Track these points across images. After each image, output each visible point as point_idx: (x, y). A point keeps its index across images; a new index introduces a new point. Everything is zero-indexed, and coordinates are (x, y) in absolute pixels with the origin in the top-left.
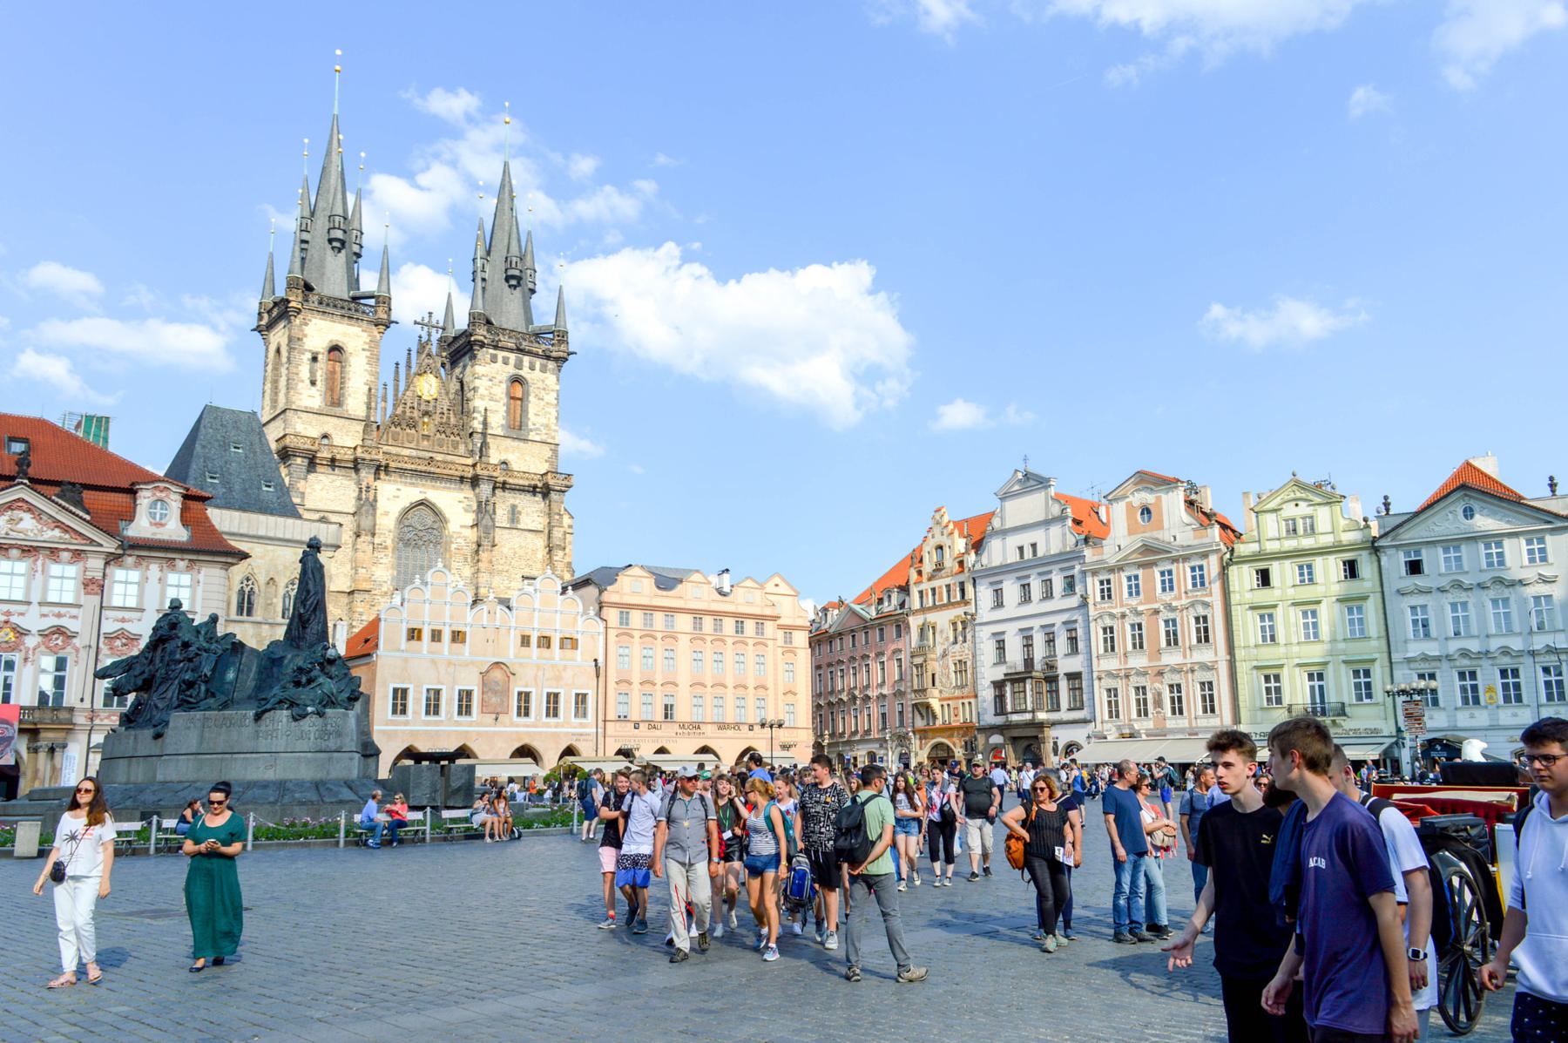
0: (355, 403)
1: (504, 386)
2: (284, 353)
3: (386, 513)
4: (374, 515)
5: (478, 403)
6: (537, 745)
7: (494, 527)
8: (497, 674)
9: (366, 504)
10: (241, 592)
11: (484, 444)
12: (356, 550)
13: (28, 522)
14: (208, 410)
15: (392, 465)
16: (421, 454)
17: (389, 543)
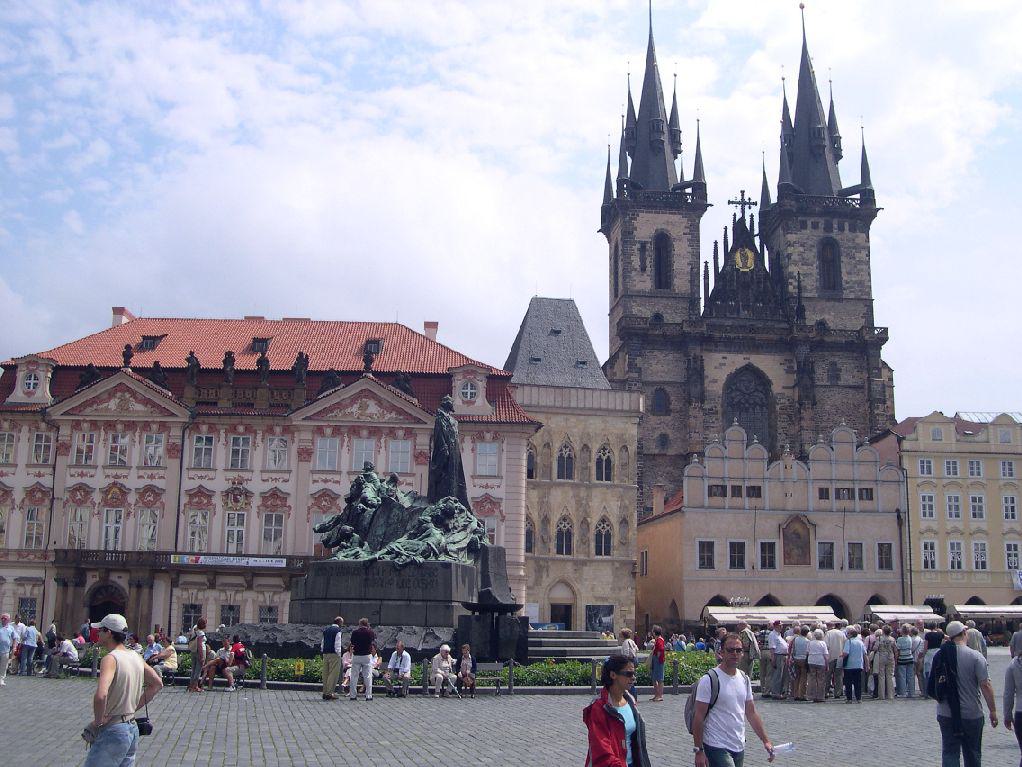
0: (680, 284)
1: (815, 250)
2: (620, 248)
3: (715, 381)
4: (702, 384)
5: (793, 269)
6: (839, 592)
7: (813, 386)
8: (797, 526)
9: (696, 373)
10: (561, 458)
11: (801, 312)
12: (689, 417)
13: (373, 408)
14: (537, 304)
15: (717, 335)
16: (742, 323)
17: (719, 408)
